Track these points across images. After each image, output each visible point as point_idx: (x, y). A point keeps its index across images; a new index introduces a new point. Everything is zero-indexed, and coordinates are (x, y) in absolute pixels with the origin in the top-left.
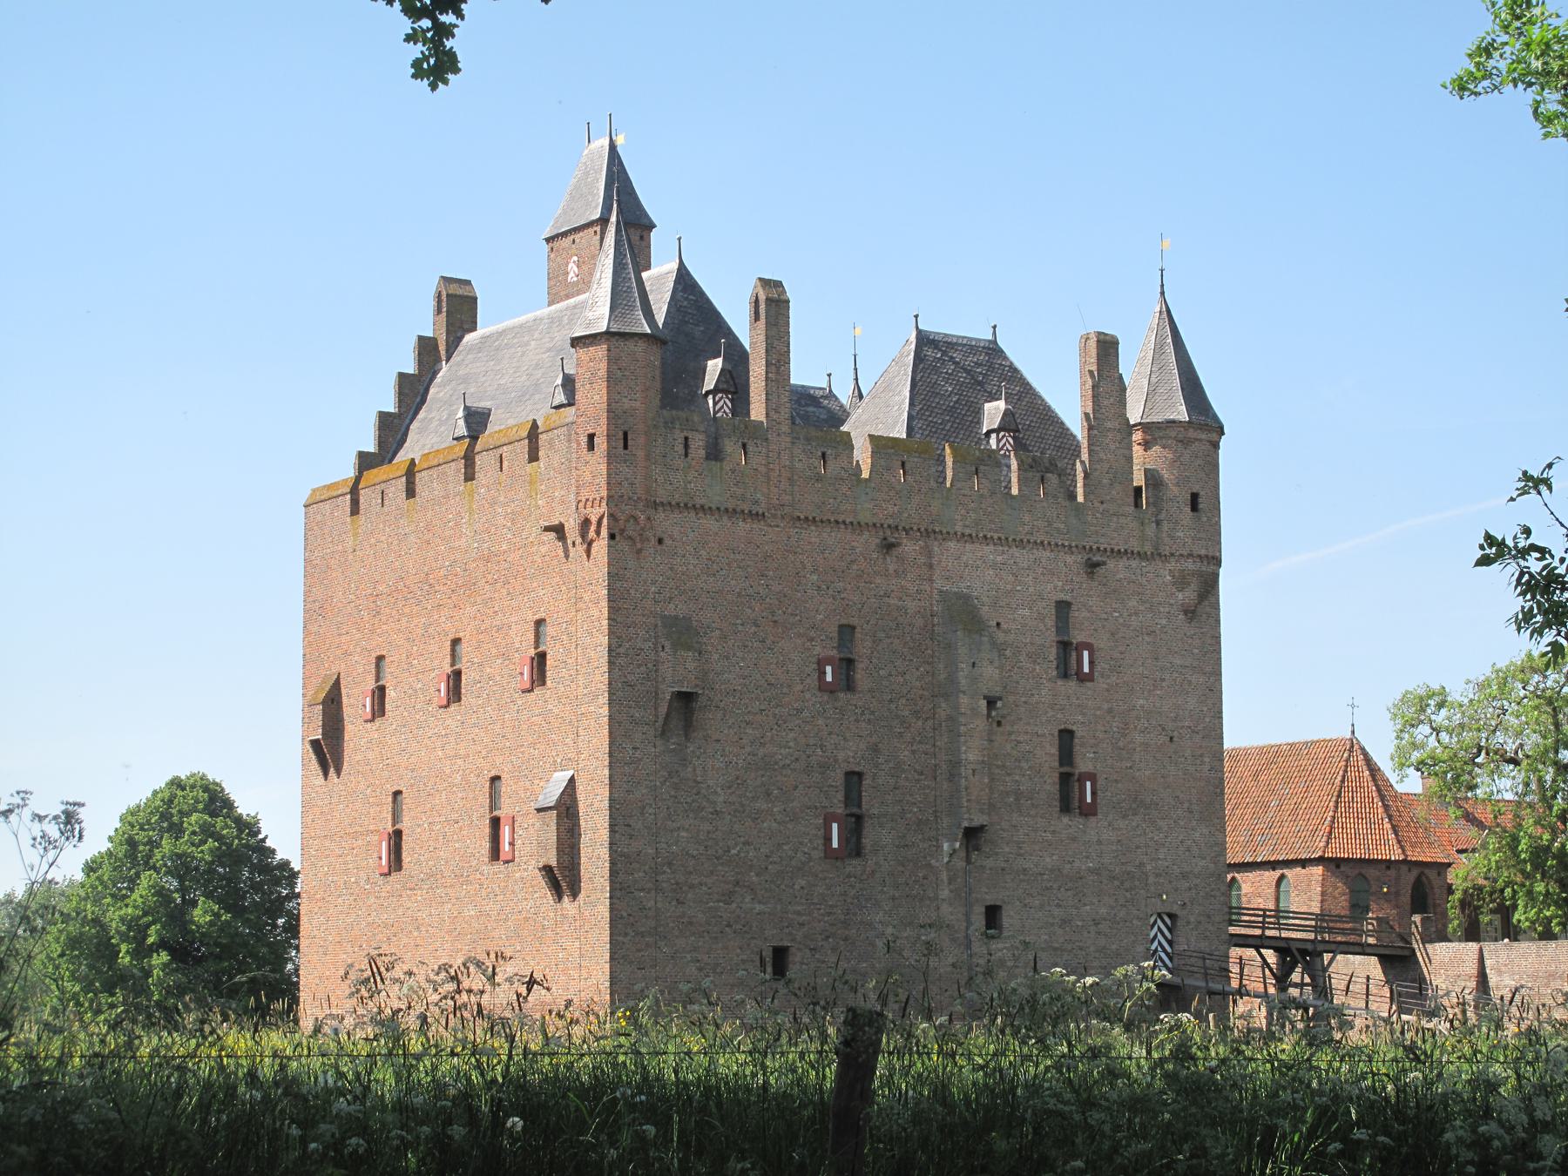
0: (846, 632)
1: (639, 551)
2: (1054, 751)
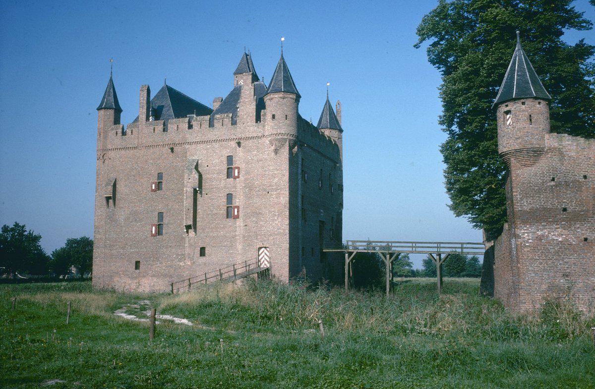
0: (160, 176)
1: (104, 162)
2: (225, 200)
